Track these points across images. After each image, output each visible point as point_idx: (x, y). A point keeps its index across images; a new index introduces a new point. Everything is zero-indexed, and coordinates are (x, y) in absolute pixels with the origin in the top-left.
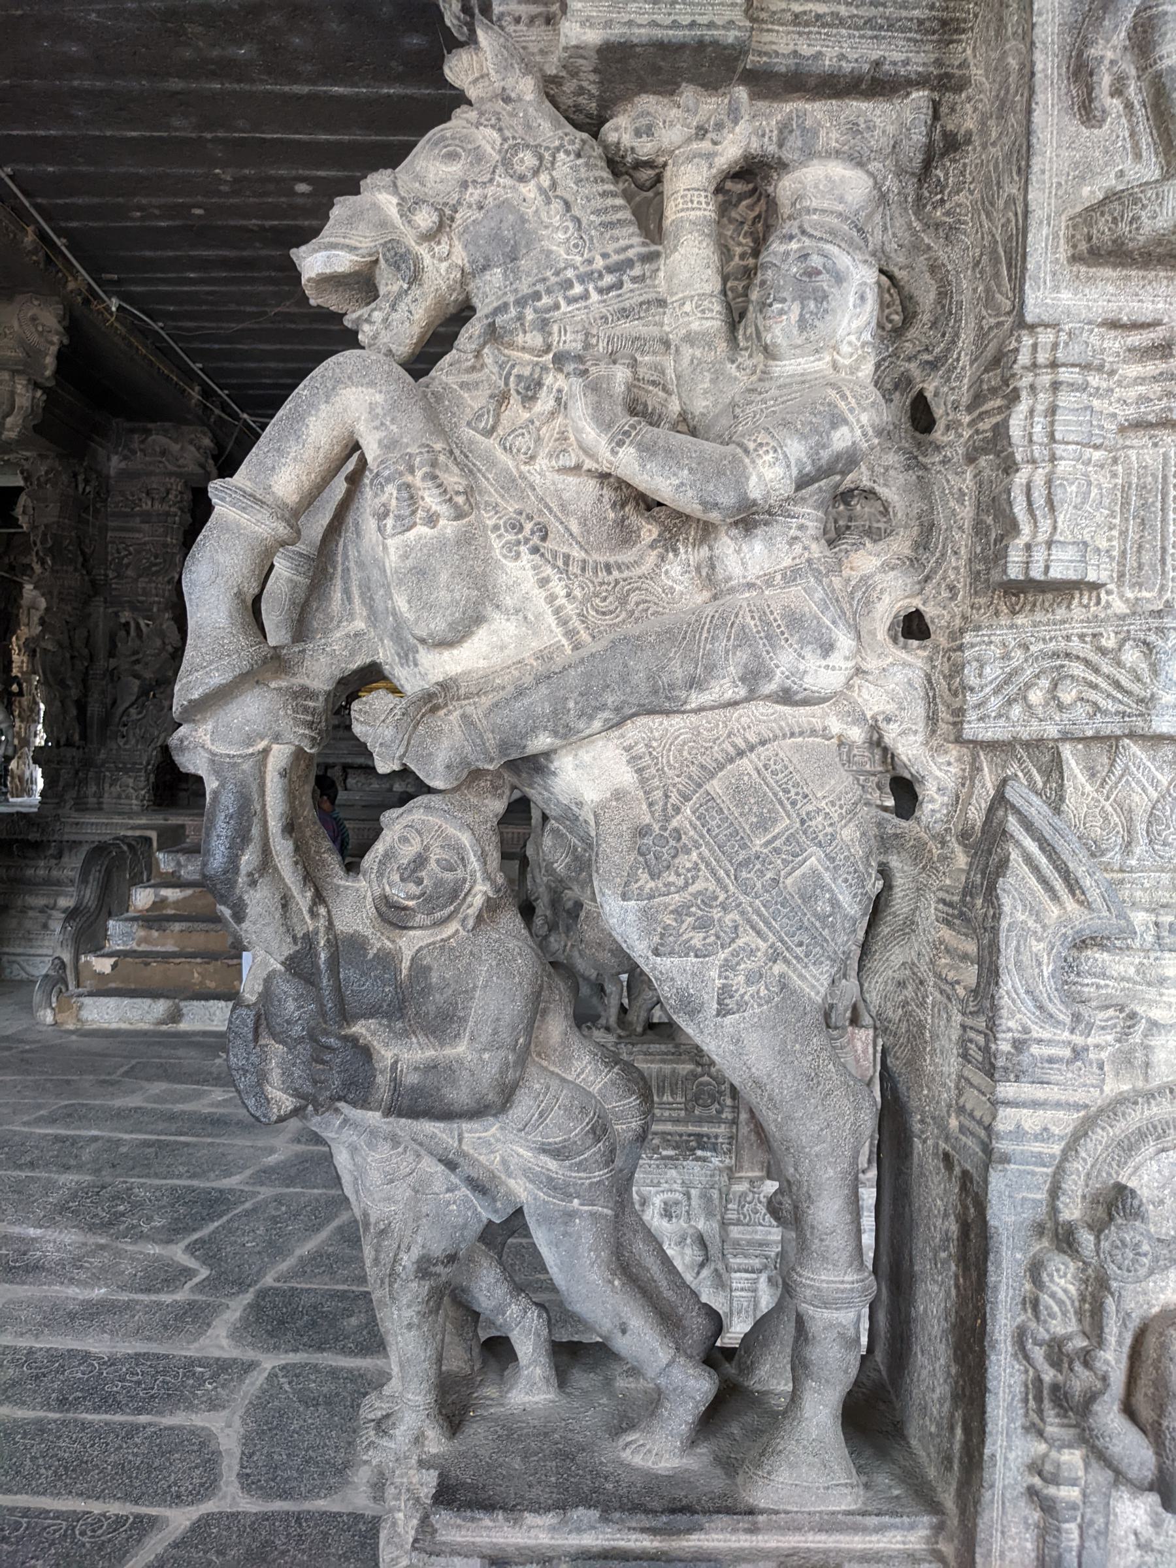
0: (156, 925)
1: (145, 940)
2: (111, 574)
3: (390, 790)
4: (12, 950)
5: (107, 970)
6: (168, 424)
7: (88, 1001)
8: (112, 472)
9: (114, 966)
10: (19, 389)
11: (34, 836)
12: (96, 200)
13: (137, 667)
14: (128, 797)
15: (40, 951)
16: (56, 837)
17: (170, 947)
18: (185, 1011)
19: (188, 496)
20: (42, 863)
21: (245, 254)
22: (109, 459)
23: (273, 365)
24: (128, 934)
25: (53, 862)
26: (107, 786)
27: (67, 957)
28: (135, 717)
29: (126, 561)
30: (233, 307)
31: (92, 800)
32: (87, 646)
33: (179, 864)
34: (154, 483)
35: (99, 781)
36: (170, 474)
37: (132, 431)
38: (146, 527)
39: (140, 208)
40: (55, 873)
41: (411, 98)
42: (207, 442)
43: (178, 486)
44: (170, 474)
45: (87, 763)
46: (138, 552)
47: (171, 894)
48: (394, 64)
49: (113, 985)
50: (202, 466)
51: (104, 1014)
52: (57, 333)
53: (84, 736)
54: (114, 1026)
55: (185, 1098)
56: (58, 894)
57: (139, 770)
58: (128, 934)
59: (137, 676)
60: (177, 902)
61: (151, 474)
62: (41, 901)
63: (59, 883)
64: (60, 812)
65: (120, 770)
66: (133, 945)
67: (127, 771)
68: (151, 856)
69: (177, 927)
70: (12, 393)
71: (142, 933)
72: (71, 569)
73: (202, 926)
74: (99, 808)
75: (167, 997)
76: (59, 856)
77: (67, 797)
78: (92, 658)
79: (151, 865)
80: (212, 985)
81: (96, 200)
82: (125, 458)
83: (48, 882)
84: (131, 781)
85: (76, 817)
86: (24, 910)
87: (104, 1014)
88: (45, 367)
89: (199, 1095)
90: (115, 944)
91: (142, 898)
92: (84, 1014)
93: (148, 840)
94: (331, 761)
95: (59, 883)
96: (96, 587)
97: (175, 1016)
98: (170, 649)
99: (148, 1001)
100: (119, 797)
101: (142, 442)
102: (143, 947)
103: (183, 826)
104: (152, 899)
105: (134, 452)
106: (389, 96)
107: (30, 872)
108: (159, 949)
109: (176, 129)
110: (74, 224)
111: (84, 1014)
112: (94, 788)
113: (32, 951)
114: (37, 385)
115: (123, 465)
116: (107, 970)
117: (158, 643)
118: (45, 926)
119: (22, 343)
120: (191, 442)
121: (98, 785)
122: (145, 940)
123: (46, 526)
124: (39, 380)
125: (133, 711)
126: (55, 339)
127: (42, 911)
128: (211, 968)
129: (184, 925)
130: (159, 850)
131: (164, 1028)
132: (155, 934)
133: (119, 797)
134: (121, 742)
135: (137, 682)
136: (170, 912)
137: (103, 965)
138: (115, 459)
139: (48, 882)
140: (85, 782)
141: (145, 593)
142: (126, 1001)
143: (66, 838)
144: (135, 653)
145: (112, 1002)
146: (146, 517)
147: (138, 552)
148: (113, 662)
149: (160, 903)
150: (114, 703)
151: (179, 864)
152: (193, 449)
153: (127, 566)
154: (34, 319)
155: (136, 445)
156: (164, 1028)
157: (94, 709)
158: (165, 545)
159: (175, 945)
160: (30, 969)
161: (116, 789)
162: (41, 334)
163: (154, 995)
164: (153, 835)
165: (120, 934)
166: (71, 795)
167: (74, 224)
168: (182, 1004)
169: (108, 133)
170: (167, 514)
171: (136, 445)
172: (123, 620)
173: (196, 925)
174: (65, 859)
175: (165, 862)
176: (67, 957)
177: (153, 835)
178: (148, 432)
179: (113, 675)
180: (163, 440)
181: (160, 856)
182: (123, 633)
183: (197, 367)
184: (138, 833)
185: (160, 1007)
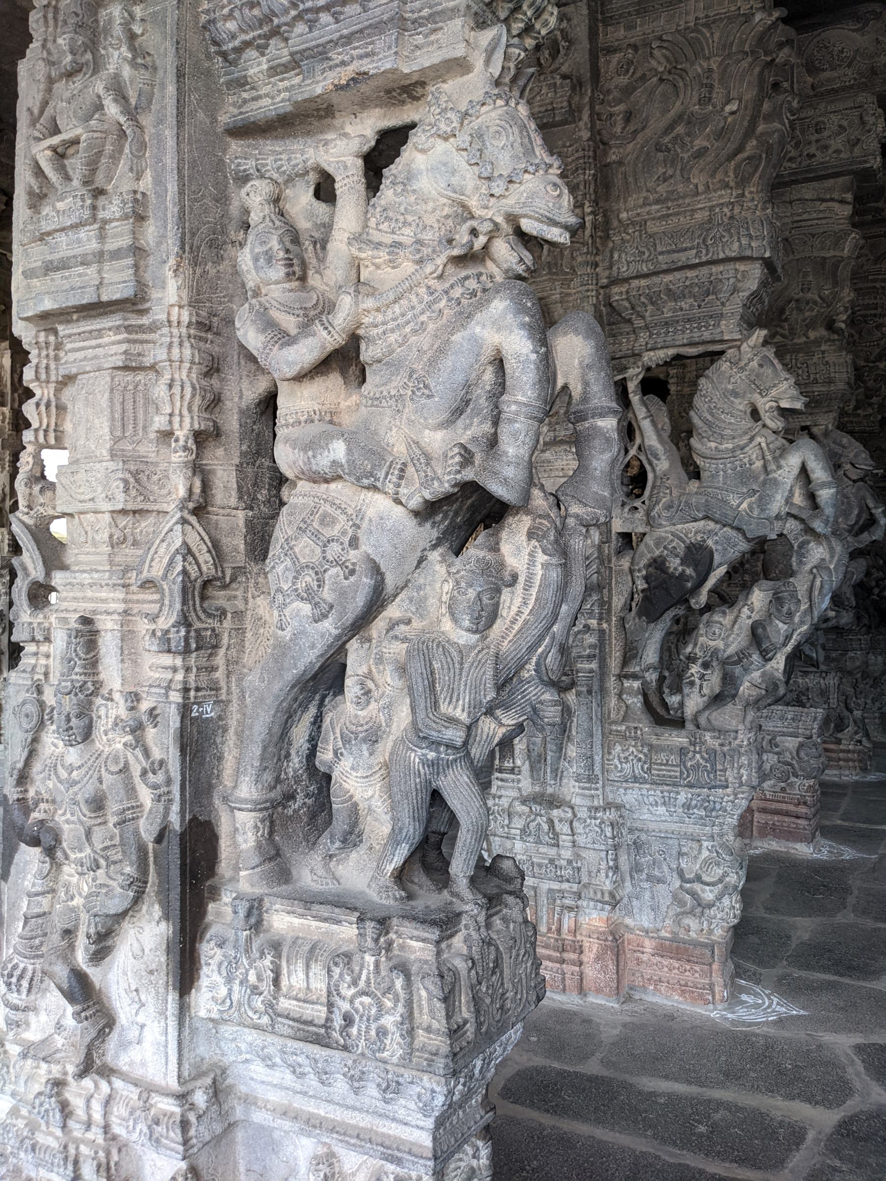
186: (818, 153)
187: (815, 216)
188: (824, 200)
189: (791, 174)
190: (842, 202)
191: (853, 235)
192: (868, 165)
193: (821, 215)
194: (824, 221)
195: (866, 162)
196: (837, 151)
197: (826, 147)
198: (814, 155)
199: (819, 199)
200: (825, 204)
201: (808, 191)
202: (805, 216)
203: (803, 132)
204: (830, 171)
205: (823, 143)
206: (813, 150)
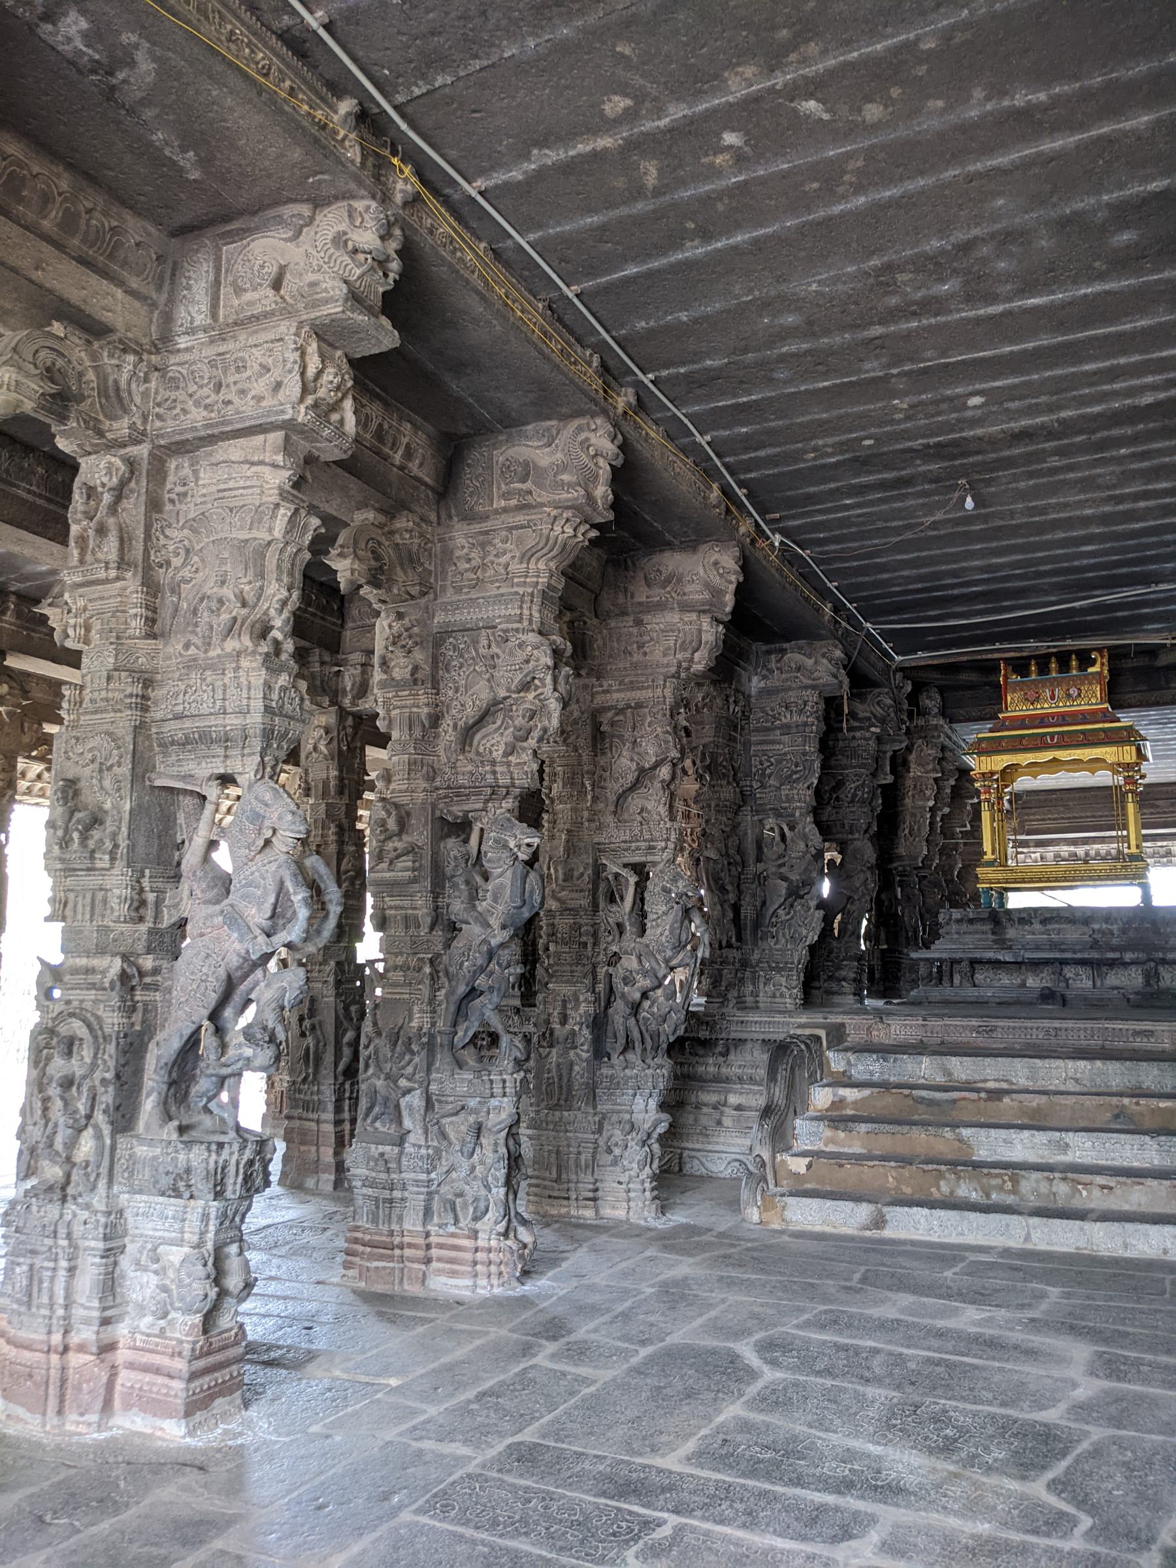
0: (842, 1125)
1: (832, 1141)
2: (755, 785)
3: (1023, 985)
4: (690, 1145)
5: (803, 1170)
6: (802, 642)
7: (791, 1200)
8: (754, 692)
9: (809, 1167)
10: (705, 626)
11: (704, 1034)
12: (778, 449)
13: (782, 870)
14: (782, 996)
15: (717, 1148)
16: (724, 1035)
17: (857, 1149)
18: (888, 1217)
19: (822, 706)
21: (903, 473)
22: (750, 680)
23: (906, 573)
24: (815, 1134)
27: (766, 1156)
28: (784, 918)
30: (880, 524)
31: (749, 999)
33: (849, 1062)
34: (792, 696)
35: (755, 980)
36: (806, 687)
37: (769, 652)
38: (786, 738)
39: (815, 450)
41: (1108, 293)
42: (838, 653)
43: (812, 697)
44: (806, 687)
45: (745, 964)
46: (779, 762)
47: (851, 1094)
48: (1097, 264)
49: (809, 1186)
50: (835, 676)
51: (808, 1215)
52: (735, 573)
53: (739, 938)
54: (818, 1228)
55: (942, 1313)
56: (729, 1091)
57: (791, 969)
58: (815, 1134)
59: (784, 878)
60: (855, 1102)
61: (789, 689)
62: (712, 1098)
63: (728, 1080)
65: (772, 969)
66: (820, 1146)
67: (779, 970)
68: (822, 1054)
69: (863, 1127)
70: (700, 631)
71: (829, 1133)
72: (724, 782)
73: (888, 1127)
74: (756, 1008)
75: (869, 1202)
76: (725, 1054)
77: (729, 996)
78: (744, 864)
79: (823, 1064)
80: (908, 1191)
81: (778, 449)
82: (764, 677)
83: (717, 1079)
84: (783, 980)
85: (740, 1015)
86: (698, 1106)
87: (808, 1215)
88: (726, 605)
89: (955, 1312)
90: (801, 1145)
91: (821, 1097)
92: (788, 1214)
93: (819, 1038)
94: (958, 956)
95: (728, 1080)
96: (744, 797)
97: (879, 1222)
98: (814, 852)
99: (851, 1204)
100: (774, 996)
101: (778, 661)
102: (831, 1148)
103: (843, 1025)
104: (830, 1098)
105: (771, 671)
106: (1085, 295)
107: (701, 1069)
108: (846, 1150)
109: (867, 371)
110: (753, 475)
111: (788, 1214)
113: (710, 1147)
114: (718, 621)
115: (762, 684)
116: (803, 1170)
117: (802, 846)
118: (719, 1123)
119: (707, 585)
120: (823, 656)
122: (832, 1141)
124: (720, 616)
125: (781, 912)
126: (733, 578)
127: (715, 1108)
128: (906, 1172)
129: (870, 1126)
130: (829, 1048)
131: (868, 1233)
132: (842, 1135)
134: (772, 942)
135: (785, 884)
136: (850, 1112)
137: (799, 1165)
138: (755, 679)
139: (717, 1079)
141: (789, 800)
142: (829, 1203)
143: (733, 1035)
145: (815, 1203)
146: (786, 729)
147: (779, 762)
148: (760, 867)
149: (839, 1104)
150: (764, 903)
151: (849, 1062)
152: (825, 661)
154: (716, 563)
155: (773, 665)
156: (868, 1233)
157: (747, 912)
158: (804, 754)
159: (862, 1146)
160: (708, 1165)
161: (770, 988)
162: (721, 575)
163: (857, 1199)
164: (822, 1033)
165: (807, 1133)
166: (733, 994)
167: (753, 475)
168: (885, 1209)
169: (803, 388)
170: (805, 724)
171: (773, 665)
173: (882, 1126)
174: (732, 1057)
175: (836, 1061)
176: (766, 1156)
177: (822, 1033)
178: (783, 651)
179: (761, 879)
180: (798, 657)
181: (830, 1054)
183: (831, 586)
184: (807, 1032)
185: (864, 1211)
186: (236, 400)
187: (242, 483)
188: (253, 464)
189: (207, 426)
190: (275, 466)
191: (282, 511)
192: (287, 417)
193: (249, 483)
194: (250, 491)
195: (283, 412)
196: (259, 399)
197: (243, 392)
198: (229, 402)
199: (246, 462)
200: (254, 469)
201: (234, 450)
202: (231, 484)
203: (225, 373)
204: (247, 424)
205: (239, 386)
206: (232, 396)
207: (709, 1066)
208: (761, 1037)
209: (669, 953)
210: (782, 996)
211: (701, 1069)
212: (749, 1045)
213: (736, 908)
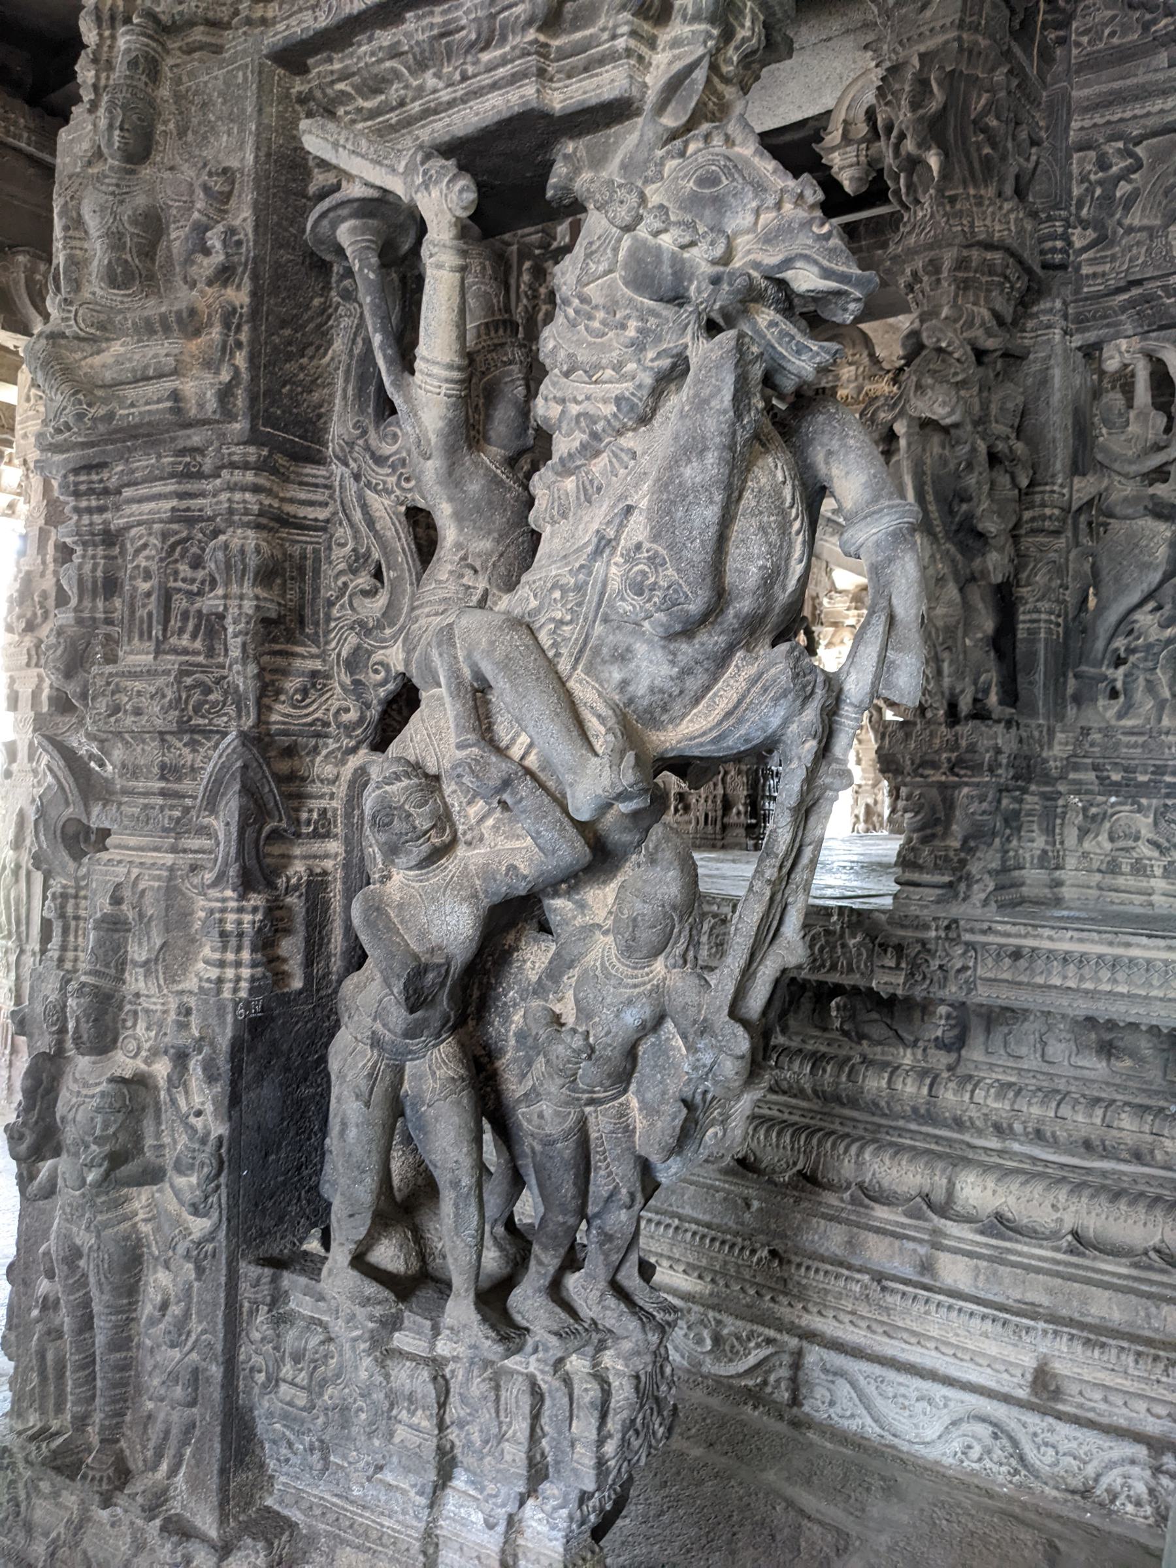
2: (1079, 238)
11: (887, 980)
14: (1139, 869)
16: (952, 991)
20: (907, 1058)
25: (941, 1060)
26: (1071, 835)
29: (1123, 189)
31: (1033, 878)
32: (1019, 431)
35: (1051, 820)
40: (950, 1097)
45: (1027, 770)
53: (1011, 696)
64: (956, 910)
67: (1130, 791)
76: (957, 1043)
77: (974, 868)
84: (1144, 824)
85: (1009, 932)
100: (1113, 868)
107: (874, 1083)
112: (1040, 842)
121: (1050, 831)
123: (922, 57)
125: (1145, 619)
133: (1113, 868)
134: (1108, 710)
140: (1013, 821)
143: (983, 995)
144: (1158, 448)
148: (1084, 488)
153: (1129, 202)
157: (1038, 617)
161: (1100, 845)
166: (985, 861)
172: (1112, 365)
174: (975, 1053)
179: (1094, 516)
182: (1115, 398)
207: (898, 1077)
208: (1082, 1007)
209: (651, 668)
210: (1139, 869)
211: (874, 1083)
212: (1032, 1026)
213: (1005, 600)
